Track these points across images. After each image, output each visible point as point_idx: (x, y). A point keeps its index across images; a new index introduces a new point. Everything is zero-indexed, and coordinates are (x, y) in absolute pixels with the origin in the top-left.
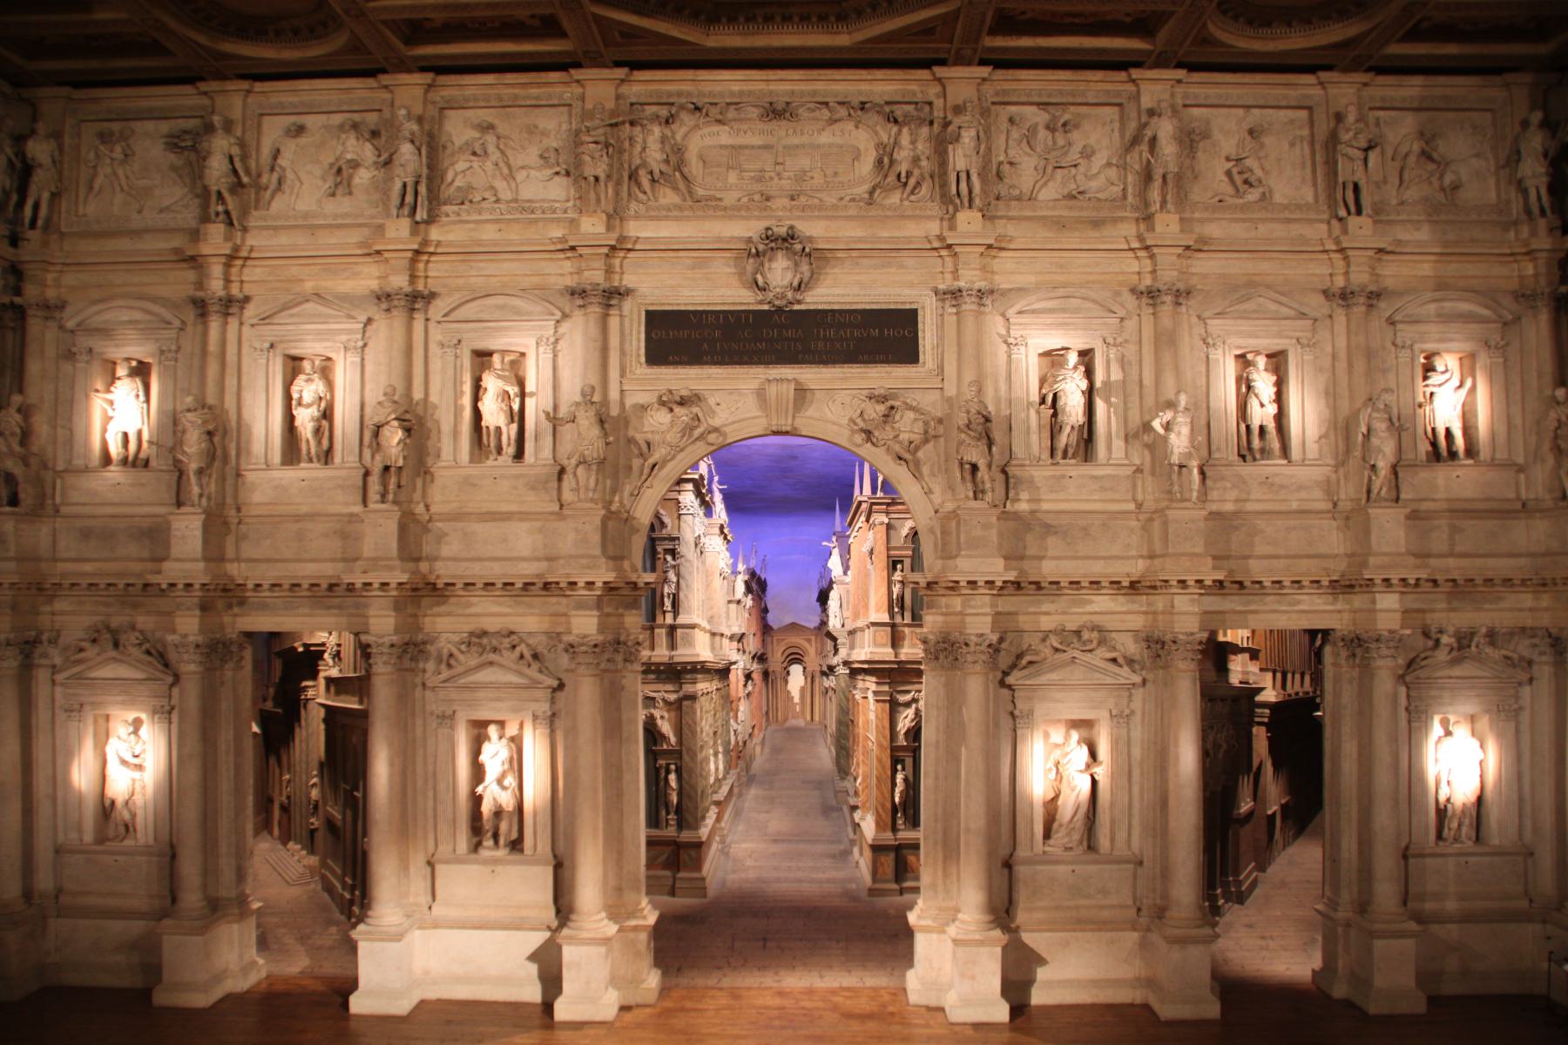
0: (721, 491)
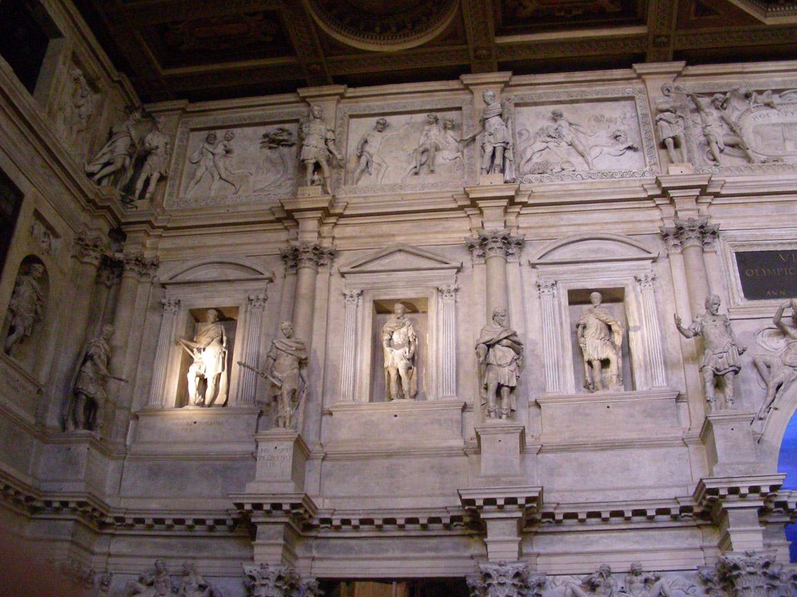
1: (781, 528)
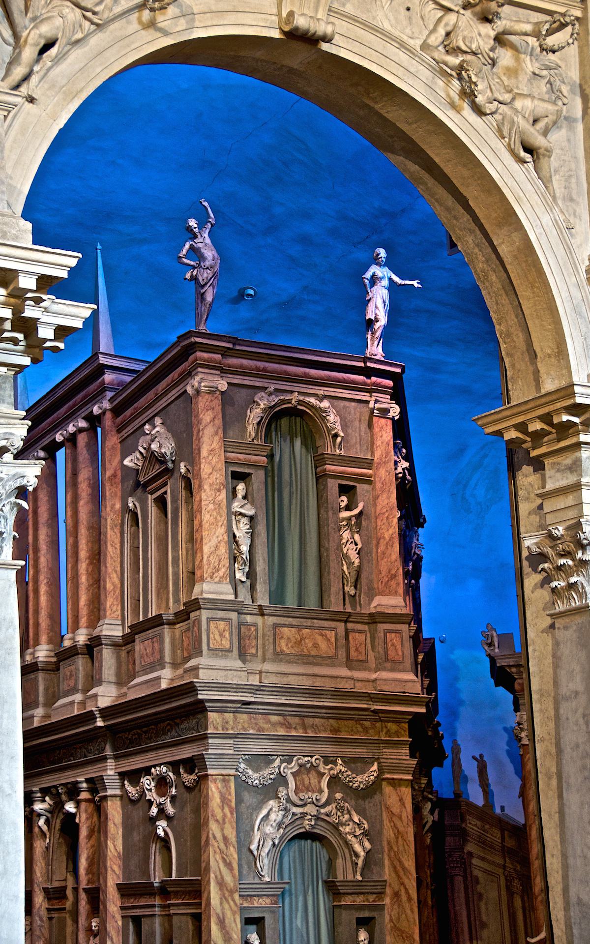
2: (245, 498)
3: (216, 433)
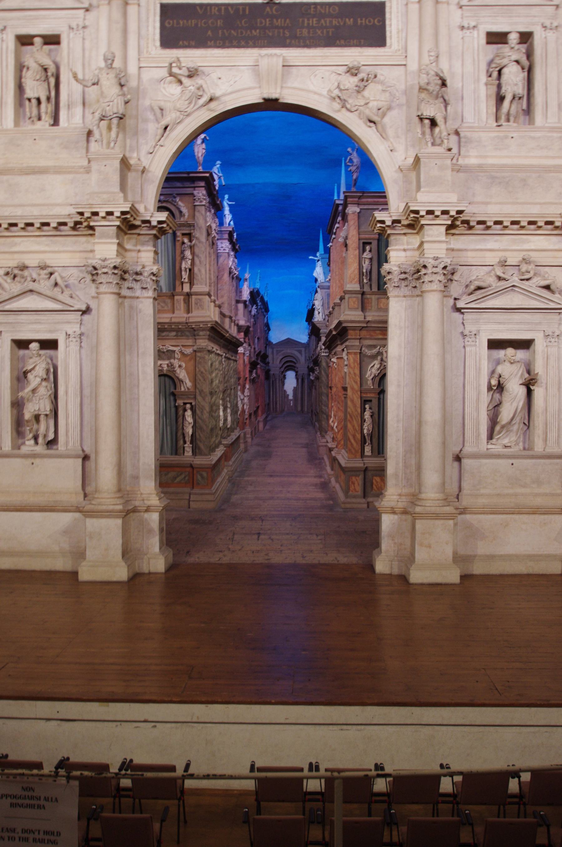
0: (229, 205)
1: (150, 238)
2: (370, 251)
3: (355, 228)
